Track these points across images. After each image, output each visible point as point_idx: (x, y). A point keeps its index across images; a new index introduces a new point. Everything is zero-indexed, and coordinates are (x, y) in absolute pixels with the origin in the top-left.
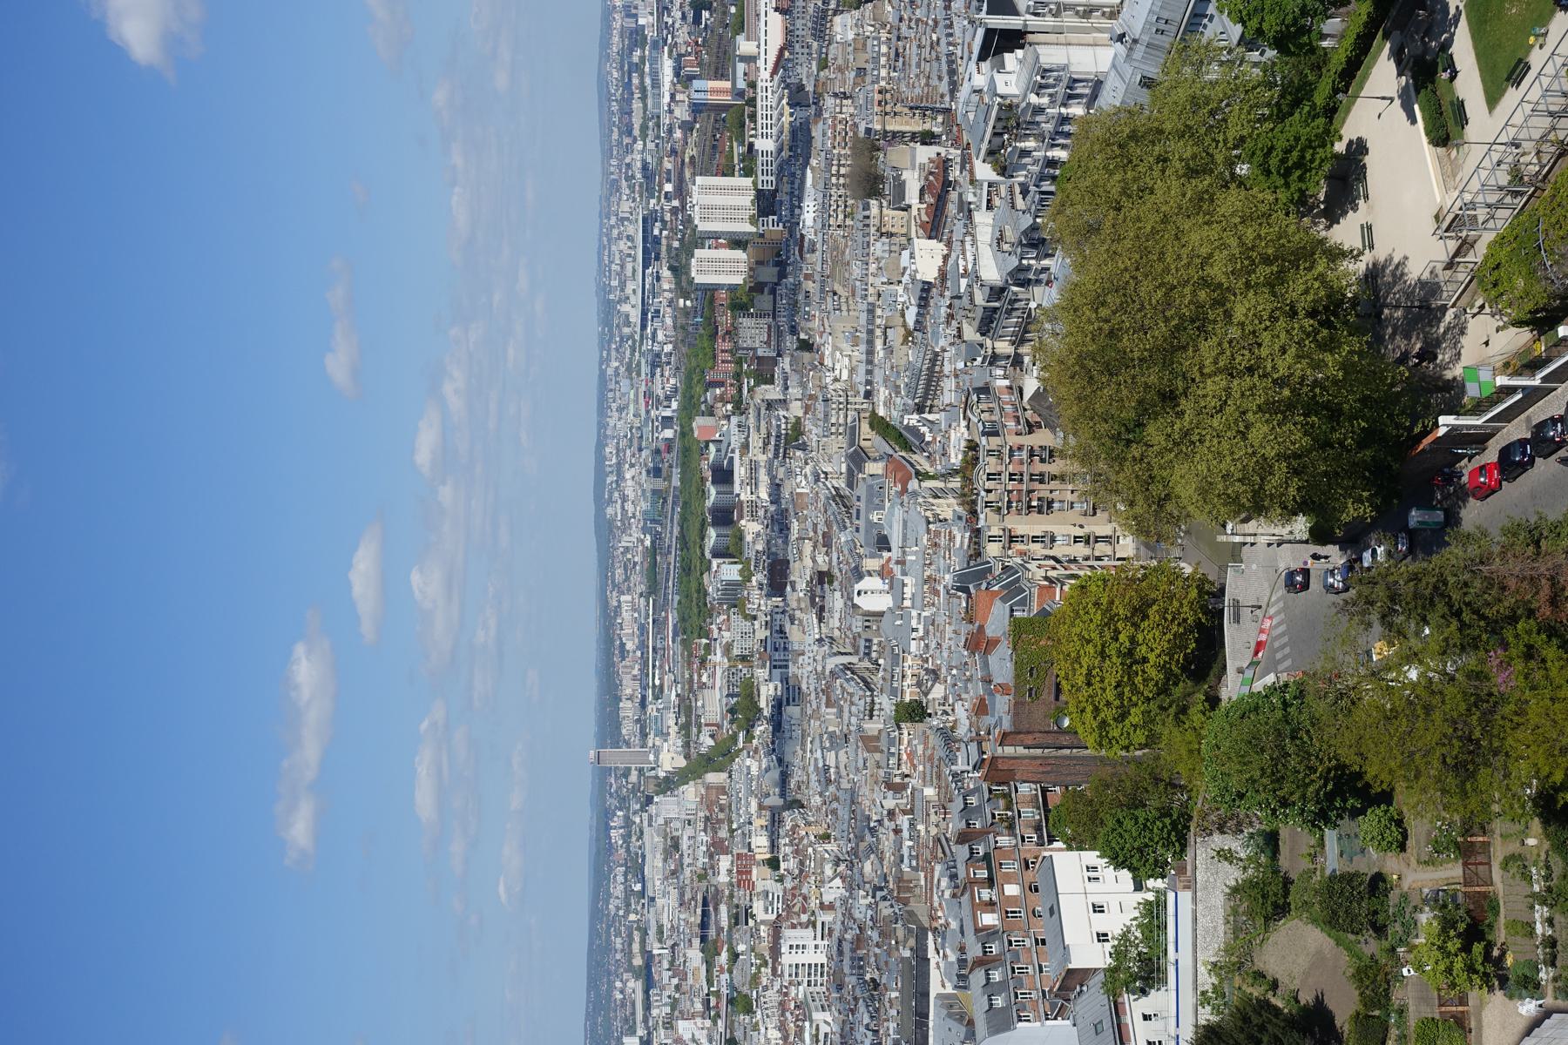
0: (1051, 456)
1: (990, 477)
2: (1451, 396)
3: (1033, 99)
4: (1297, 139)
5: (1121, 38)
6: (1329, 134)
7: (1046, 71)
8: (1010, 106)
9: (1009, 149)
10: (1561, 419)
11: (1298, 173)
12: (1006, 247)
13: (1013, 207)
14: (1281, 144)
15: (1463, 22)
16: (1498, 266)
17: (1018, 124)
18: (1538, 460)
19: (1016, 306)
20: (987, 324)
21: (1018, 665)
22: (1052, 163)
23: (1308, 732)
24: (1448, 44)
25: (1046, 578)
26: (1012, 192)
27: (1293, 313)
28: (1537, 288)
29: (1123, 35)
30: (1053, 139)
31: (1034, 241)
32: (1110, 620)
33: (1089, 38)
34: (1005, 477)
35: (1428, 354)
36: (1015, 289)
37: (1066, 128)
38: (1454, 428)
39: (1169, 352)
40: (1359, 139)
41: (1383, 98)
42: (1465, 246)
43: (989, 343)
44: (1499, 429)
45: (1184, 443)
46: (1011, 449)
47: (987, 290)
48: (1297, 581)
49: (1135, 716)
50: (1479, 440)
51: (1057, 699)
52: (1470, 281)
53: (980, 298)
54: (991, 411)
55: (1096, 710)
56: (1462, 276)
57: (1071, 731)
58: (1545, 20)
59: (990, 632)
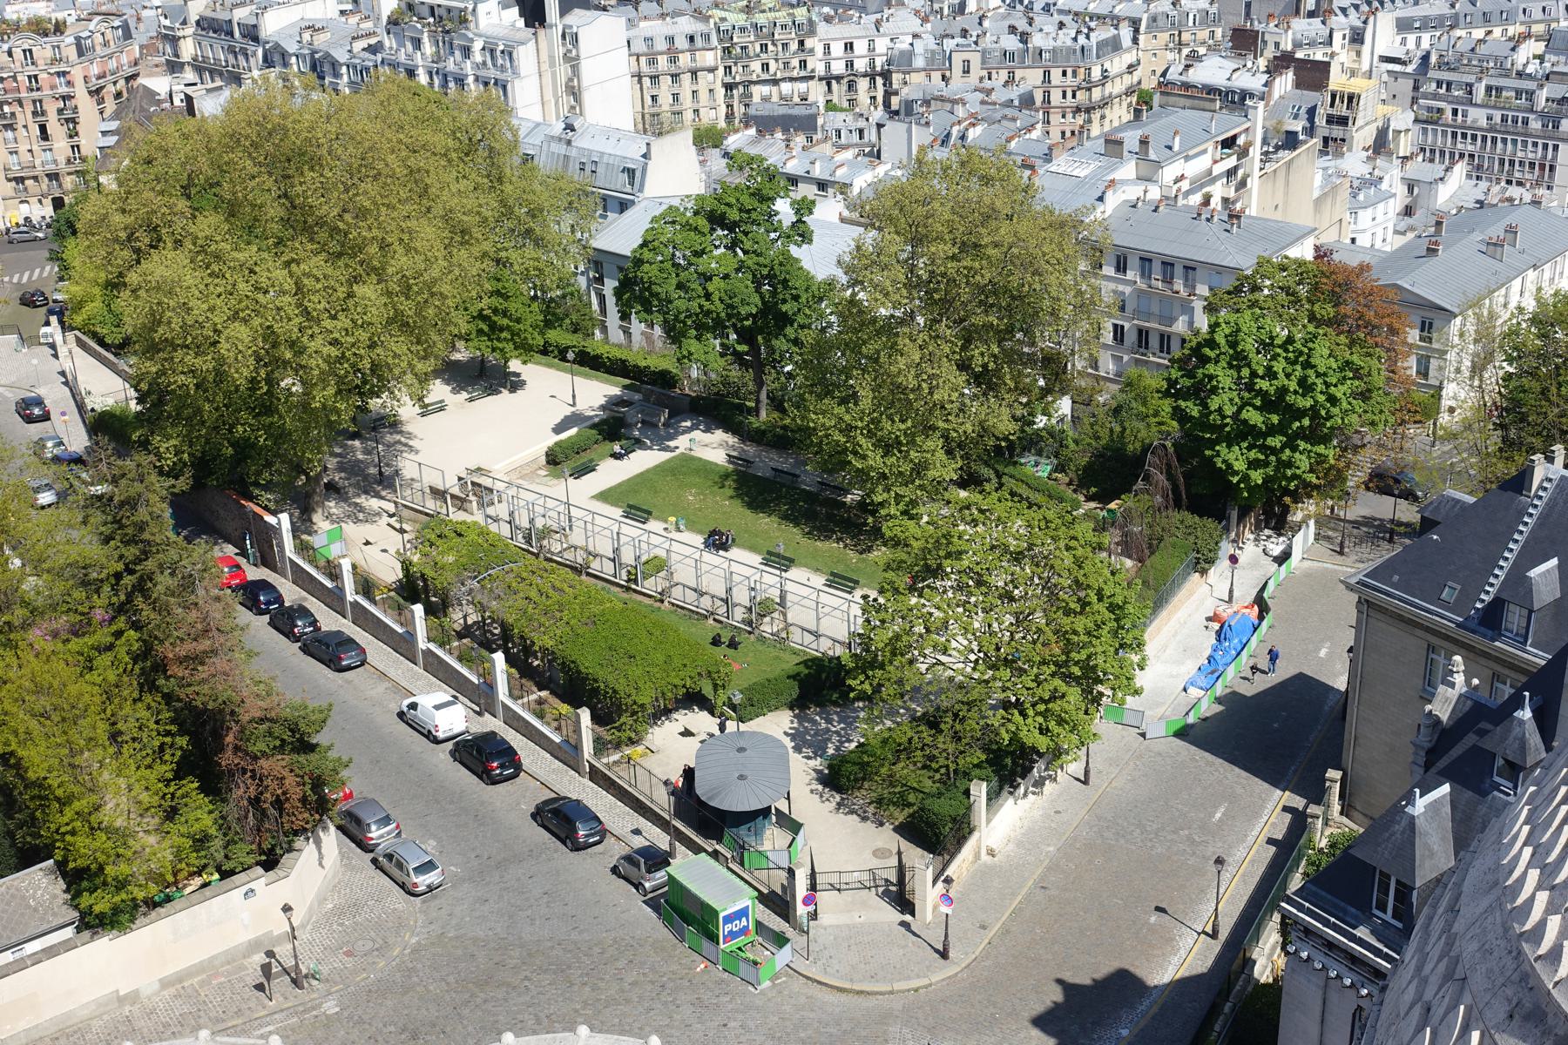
0: (67, 120)
1: (28, 53)
2: (302, 526)
3: (478, 45)
4: (518, 321)
5: (570, 127)
6: (526, 350)
7: (510, 54)
8: (466, 21)
9: (419, 26)
10: (317, 629)
11: (486, 328)
12: (306, 36)
13: (353, 38)
14: (514, 306)
15: (667, 455)
16: (460, 535)
17: (448, 32)
18: (267, 618)
19: (240, 57)
20: (207, 25)
22: (411, 73)
24: (639, 444)
26: (369, 35)
27: (372, 346)
28: (450, 576)
29: (573, 130)
30: (437, 73)
31: (321, 66)
33: (549, 96)
34: (31, 70)
35: (332, 488)
36: (260, 52)
37: (452, 85)
38: (276, 531)
40: (523, 383)
41: (574, 396)
42: (461, 503)
43: (190, 30)
44: (284, 575)
45: (206, 257)
46: (64, 74)
47: (253, 21)
50: (267, 560)
52: (427, 514)
54: (106, 44)
56: (431, 505)
58: (692, 527)
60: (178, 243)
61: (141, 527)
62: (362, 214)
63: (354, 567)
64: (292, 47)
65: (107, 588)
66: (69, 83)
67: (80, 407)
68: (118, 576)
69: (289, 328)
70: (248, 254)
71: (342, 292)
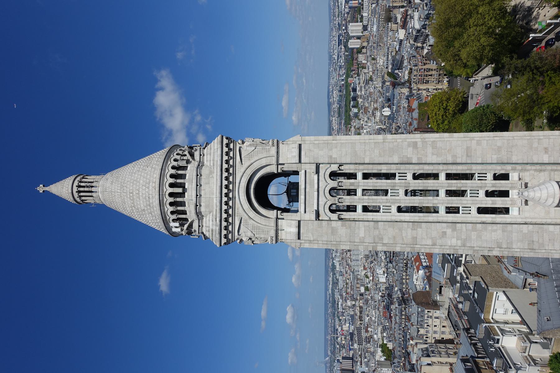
0: (429, 70)
18: (556, 42)
20: (415, 40)
21: (419, 113)
23: (489, 115)
25: (427, 95)
26: (423, 6)
27: (494, 10)
31: (428, 17)
32: (441, 102)
34: (418, 76)
38: (534, 37)
39: (461, 24)
44: (546, 37)
45: (464, 45)
46: (420, 69)
47: (416, 31)
48: (488, 87)
49: (446, 122)
51: (428, 121)
53: (414, 33)
54: (416, 61)
55: (437, 121)
57: (431, 128)
59: (413, 107)
60: (460, 51)
61: (523, 67)
62: (462, 10)
63: (550, 19)
64: (423, 23)
65: (535, 76)
66: (422, 69)
67: (490, 77)
68: (533, 73)
69: (485, 29)
70: (465, 36)
71: (479, 16)
